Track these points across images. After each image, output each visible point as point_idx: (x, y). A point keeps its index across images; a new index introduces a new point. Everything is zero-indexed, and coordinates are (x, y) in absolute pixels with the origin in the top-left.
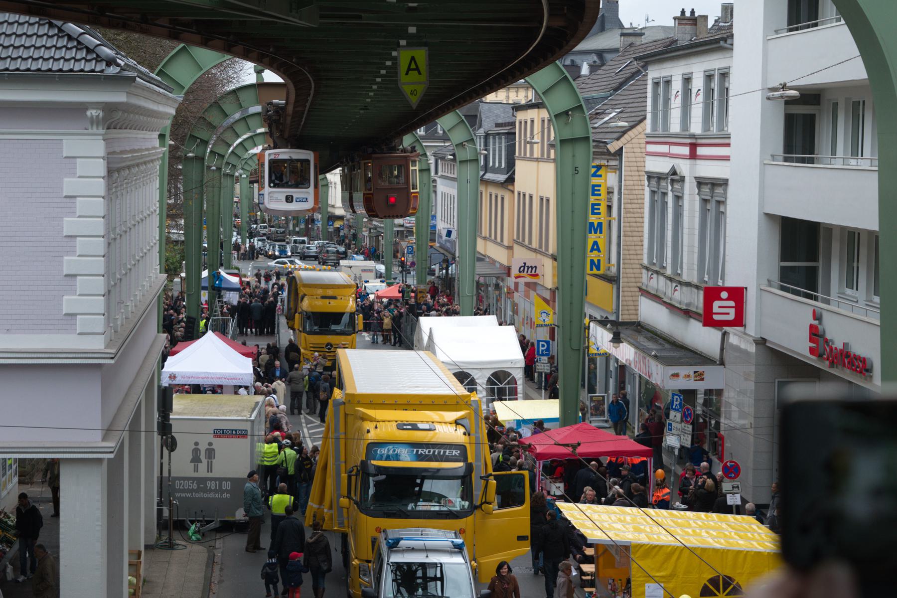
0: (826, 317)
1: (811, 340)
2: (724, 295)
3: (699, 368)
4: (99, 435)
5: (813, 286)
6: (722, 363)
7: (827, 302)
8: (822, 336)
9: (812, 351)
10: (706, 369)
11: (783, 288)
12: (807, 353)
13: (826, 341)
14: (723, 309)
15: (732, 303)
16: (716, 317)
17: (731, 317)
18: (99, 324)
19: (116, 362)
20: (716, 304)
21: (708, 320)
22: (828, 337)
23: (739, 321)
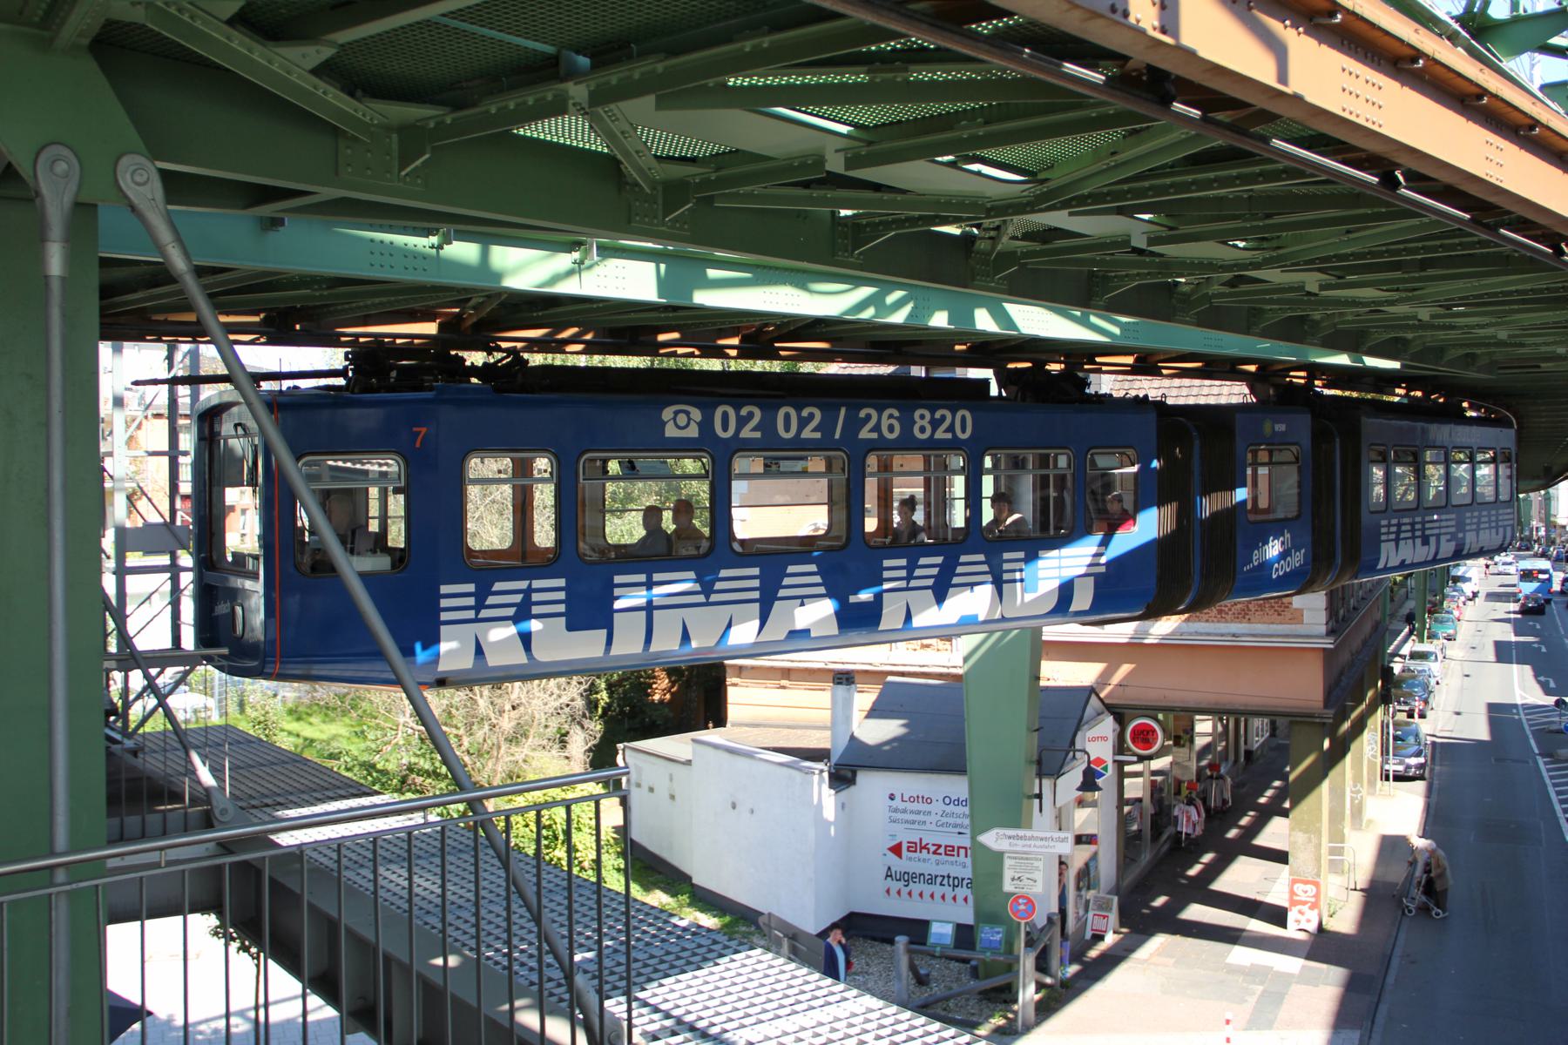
4: (1321, 705)
18: (1322, 617)
19: (1336, 648)
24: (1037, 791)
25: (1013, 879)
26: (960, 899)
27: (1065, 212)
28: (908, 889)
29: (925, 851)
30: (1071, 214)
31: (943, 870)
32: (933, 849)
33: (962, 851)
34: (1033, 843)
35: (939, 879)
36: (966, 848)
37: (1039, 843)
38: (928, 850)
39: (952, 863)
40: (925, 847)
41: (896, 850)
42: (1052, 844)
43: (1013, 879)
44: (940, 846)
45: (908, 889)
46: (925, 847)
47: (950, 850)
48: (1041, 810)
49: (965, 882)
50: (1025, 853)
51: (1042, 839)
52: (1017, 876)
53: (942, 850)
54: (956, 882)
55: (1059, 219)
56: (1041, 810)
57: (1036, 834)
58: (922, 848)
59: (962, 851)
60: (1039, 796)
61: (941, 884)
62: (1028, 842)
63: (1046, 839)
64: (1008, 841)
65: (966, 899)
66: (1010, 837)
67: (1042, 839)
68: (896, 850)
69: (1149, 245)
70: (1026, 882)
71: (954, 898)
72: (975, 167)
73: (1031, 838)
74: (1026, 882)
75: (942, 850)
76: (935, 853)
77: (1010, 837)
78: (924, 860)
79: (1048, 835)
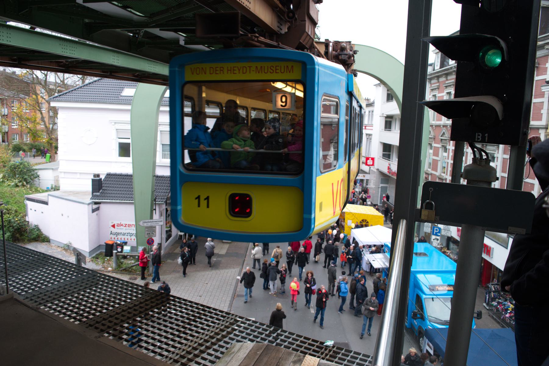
0: (391, 165)
1: (388, 170)
2: (370, 159)
3: (364, 175)
5: (389, 158)
6: (369, 174)
7: (392, 161)
8: (390, 169)
9: (388, 172)
10: (366, 175)
11: (383, 158)
12: (387, 172)
13: (391, 170)
14: (370, 162)
15: (372, 161)
16: (368, 164)
17: (371, 163)
20: (368, 161)
21: (366, 164)
22: (391, 169)
23: (373, 165)
24: (154, 208)
25: (147, 234)
26: (133, 240)
27: (158, 29)
28: (117, 237)
29: (122, 226)
30: (160, 30)
31: (128, 231)
32: (124, 225)
33: (133, 226)
34: (153, 223)
35: (126, 234)
36: (134, 225)
37: (155, 223)
38: (123, 226)
39: (130, 229)
40: (122, 225)
41: (113, 226)
42: (158, 223)
43: (147, 234)
44: (126, 225)
45: (117, 237)
46: (122, 225)
47: (130, 226)
48: (156, 213)
49: (134, 234)
50: (152, 226)
51: (155, 222)
52: (149, 233)
53: (127, 226)
54: (131, 235)
55: (156, 31)
56: (156, 213)
57: (154, 220)
58: (121, 225)
59: (133, 226)
60: (155, 210)
61: (127, 235)
62: (151, 223)
63: (156, 222)
64: (146, 223)
65: (134, 239)
66: (146, 222)
67: (155, 222)
68: (113, 226)
69: (185, 44)
70: (151, 234)
71: (131, 239)
72: (129, 10)
73: (152, 222)
74: (151, 234)
75: (127, 226)
76: (125, 226)
77: (146, 222)
78: (122, 229)
79: (159, 220)
